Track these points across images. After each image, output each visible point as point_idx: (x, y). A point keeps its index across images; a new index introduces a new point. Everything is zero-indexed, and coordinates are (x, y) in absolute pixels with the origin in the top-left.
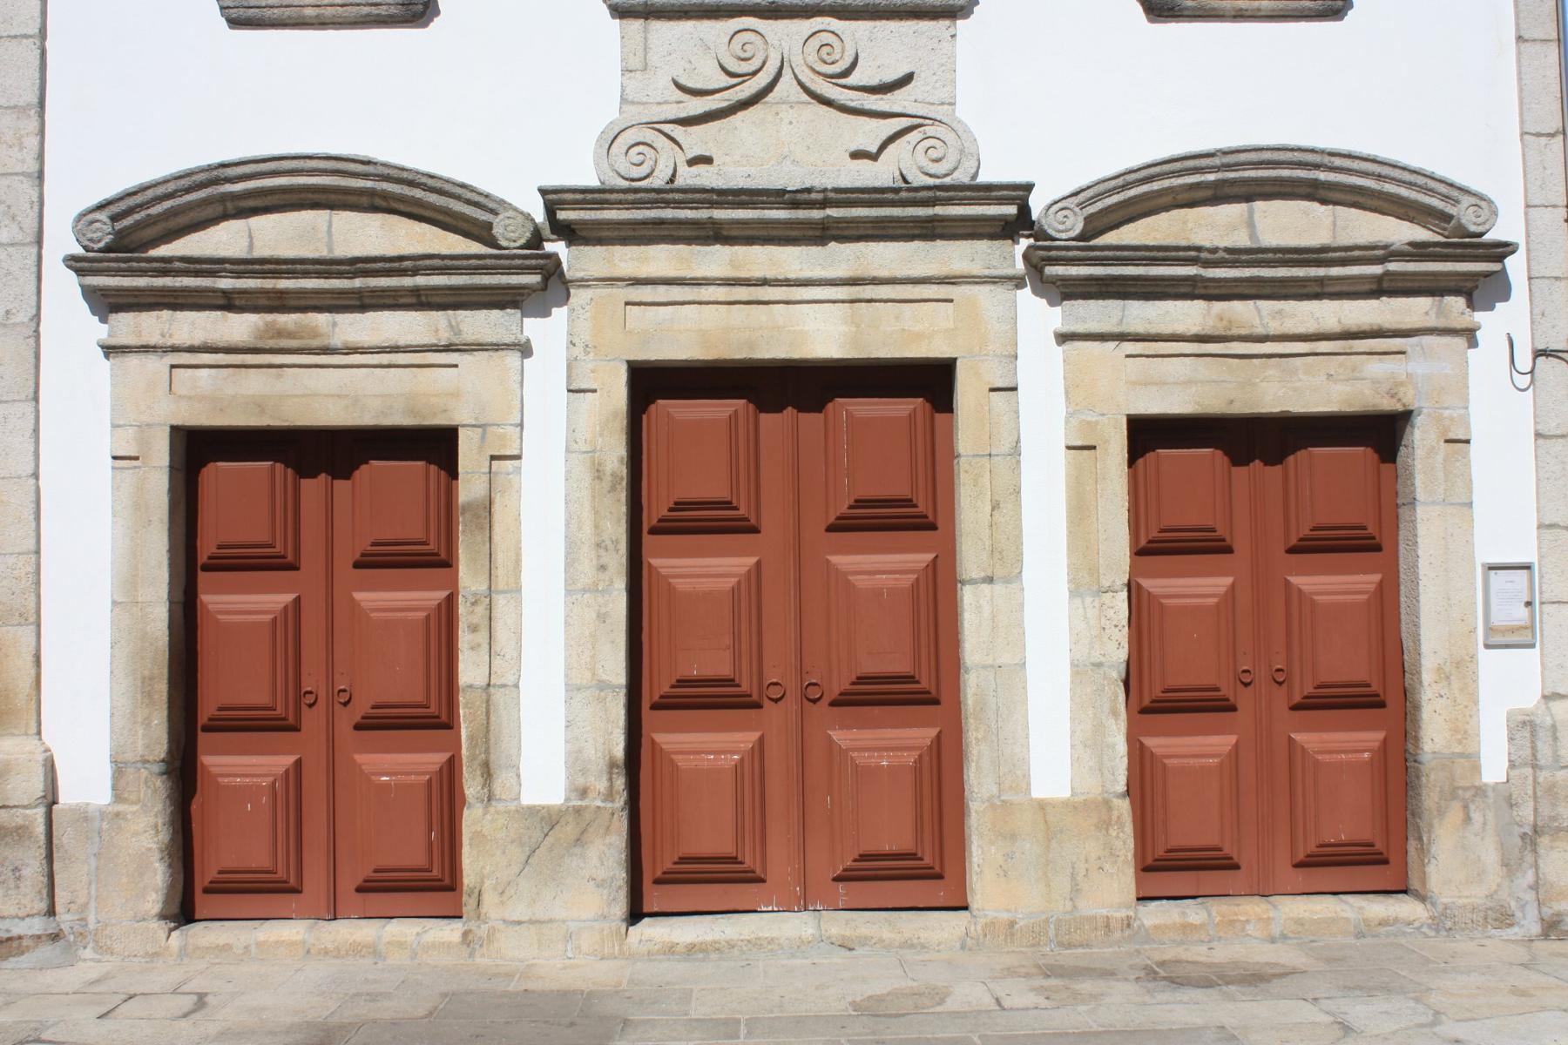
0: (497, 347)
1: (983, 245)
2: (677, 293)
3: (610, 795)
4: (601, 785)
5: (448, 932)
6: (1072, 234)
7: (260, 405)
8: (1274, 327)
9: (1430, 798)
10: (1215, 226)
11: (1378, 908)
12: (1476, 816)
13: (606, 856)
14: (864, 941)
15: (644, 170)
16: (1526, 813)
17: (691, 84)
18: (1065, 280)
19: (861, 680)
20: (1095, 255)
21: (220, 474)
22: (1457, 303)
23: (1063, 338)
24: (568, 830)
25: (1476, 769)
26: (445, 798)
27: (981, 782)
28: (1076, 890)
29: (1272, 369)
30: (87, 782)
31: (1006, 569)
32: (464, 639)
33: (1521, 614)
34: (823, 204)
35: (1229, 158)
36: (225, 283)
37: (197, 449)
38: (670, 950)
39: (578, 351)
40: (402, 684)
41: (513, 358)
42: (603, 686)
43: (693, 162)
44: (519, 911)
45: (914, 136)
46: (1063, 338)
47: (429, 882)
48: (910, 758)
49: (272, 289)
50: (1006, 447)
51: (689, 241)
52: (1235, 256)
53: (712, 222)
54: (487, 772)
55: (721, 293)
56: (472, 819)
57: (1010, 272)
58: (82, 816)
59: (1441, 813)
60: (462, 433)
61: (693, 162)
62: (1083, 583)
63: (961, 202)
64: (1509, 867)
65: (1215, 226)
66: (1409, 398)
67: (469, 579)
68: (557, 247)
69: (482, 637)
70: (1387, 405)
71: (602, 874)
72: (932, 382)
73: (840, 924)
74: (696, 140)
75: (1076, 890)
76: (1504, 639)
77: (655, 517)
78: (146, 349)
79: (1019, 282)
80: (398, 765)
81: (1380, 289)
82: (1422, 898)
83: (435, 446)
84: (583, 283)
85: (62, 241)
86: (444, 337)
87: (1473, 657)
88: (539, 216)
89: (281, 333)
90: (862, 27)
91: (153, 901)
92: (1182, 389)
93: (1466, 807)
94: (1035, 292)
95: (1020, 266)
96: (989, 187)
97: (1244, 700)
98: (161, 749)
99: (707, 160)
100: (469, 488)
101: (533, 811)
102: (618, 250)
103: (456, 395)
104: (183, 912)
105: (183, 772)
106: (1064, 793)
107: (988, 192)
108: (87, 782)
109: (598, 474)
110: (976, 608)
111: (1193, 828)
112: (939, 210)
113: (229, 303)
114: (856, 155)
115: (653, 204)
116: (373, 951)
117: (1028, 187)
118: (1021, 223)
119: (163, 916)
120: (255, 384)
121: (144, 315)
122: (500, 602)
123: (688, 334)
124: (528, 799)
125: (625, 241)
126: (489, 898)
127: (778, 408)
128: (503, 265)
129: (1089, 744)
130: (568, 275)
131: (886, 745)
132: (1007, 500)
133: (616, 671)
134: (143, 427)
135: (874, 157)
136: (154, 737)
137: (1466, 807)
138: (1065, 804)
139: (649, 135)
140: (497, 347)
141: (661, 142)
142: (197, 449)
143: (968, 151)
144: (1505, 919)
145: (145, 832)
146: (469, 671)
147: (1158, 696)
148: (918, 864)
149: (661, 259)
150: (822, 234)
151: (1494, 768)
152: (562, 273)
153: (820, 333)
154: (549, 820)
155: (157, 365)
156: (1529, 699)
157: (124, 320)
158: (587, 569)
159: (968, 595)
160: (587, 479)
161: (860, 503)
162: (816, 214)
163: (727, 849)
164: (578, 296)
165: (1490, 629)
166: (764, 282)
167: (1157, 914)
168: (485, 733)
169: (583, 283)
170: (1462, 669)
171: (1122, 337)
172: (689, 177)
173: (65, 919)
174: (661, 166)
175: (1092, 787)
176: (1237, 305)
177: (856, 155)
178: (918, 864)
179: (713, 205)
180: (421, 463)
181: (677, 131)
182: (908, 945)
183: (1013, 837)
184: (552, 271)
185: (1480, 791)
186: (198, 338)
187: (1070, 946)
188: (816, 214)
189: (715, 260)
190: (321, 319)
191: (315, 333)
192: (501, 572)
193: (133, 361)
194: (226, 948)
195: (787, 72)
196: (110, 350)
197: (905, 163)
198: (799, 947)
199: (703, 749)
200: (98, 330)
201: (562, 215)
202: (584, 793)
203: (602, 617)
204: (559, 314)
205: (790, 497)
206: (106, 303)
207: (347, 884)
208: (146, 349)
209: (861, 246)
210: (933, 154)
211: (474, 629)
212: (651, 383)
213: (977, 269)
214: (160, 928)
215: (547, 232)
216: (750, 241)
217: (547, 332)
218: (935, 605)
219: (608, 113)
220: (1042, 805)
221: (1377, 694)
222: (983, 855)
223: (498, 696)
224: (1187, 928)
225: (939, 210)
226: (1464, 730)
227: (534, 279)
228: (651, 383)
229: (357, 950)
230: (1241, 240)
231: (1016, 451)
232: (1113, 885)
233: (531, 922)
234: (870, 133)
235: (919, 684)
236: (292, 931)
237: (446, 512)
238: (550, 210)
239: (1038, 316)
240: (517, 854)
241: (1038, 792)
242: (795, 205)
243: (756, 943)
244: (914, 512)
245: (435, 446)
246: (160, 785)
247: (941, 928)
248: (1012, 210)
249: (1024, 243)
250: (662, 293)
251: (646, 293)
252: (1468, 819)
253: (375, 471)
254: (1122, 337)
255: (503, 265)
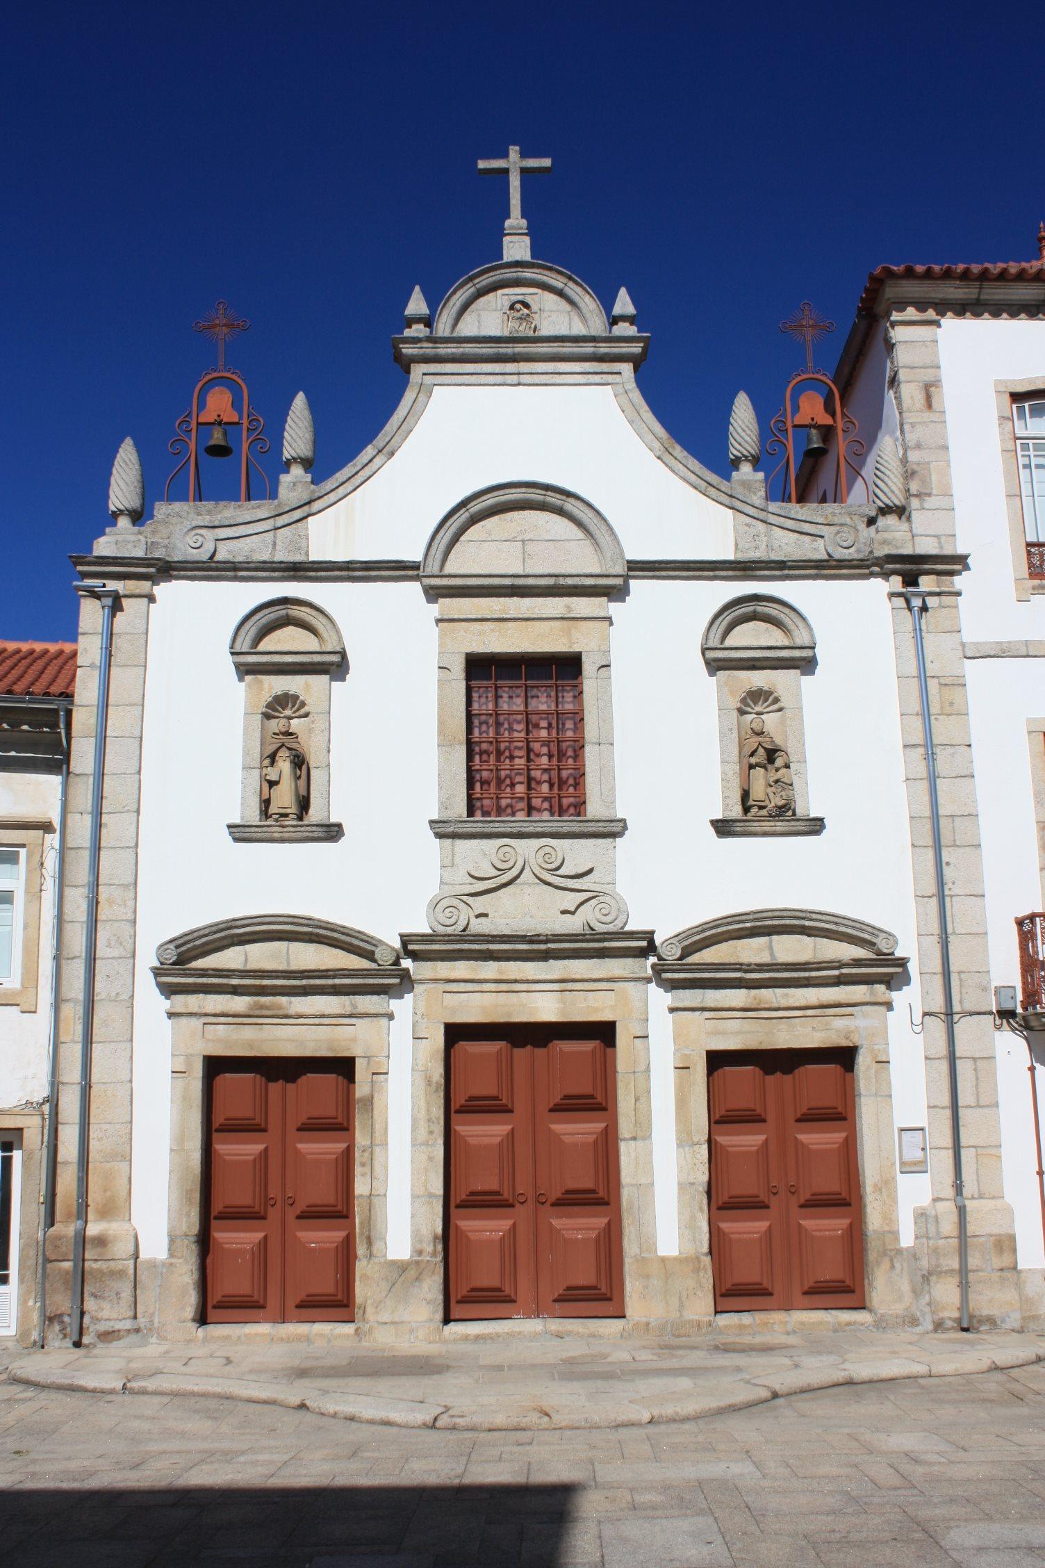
0: (376, 1015)
1: (629, 961)
2: (470, 987)
3: (434, 1254)
4: (430, 1249)
5: (348, 1329)
6: (678, 956)
7: (250, 1044)
8: (784, 1003)
9: (872, 1256)
10: (751, 951)
11: (845, 1316)
12: (897, 1265)
13: (432, 1287)
14: (569, 1333)
15: (452, 921)
16: (924, 1263)
17: (477, 875)
18: (672, 980)
19: (568, 1192)
20: (688, 967)
21: (227, 1079)
22: (881, 988)
23: (672, 1010)
24: (412, 1273)
25: (897, 1239)
26: (346, 1256)
27: (631, 1247)
28: (681, 1306)
29: (783, 1025)
30: (155, 1247)
31: (643, 1133)
32: (358, 1170)
33: (920, 1154)
34: (546, 942)
35: (757, 915)
36: (235, 982)
37: (215, 1066)
38: (466, 1338)
39: (418, 1017)
40: (322, 1193)
41: (384, 1021)
42: (431, 1195)
43: (478, 916)
44: (385, 1317)
45: (593, 902)
46: (672, 1010)
47: (338, 1303)
48: (593, 1234)
49: (258, 984)
50: (643, 1068)
51: (476, 959)
52: (761, 967)
53: (488, 950)
54: (370, 1242)
55: (493, 987)
56: (361, 1267)
57: (643, 975)
58: (152, 1264)
59: (878, 1264)
60: (358, 1061)
61: (478, 916)
62: (684, 1140)
63: (618, 940)
64: (916, 1293)
65: (751, 951)
66: (855, 1040)
67: (361, 1139)
68: (407, 963)
69: (367, 1169)
70: (844, 1043)
71: (430, 1297)
72: (604, 1032)
73: (555, 1325)
74: (479, 904)
75: (681, 1306)
76: (912, 1168)
77: (458, 1104)
78: (191, 1015)
79: (649, 980)
80: (319, 1238)
81: (839, 981)
82: (871, 1311)
83: (344, 1067)
84: (421, 981)
85: (147, 959)
86: (348, 1010)
87: (894, 1178)
88: (397, 944)
89: (262, 1007)
90: (566, 843)
91: (190, 1311)
92: (735, 1036)
93: (892, 1260)
94: (658, 985)
95: (650, 972)
96: (632, 933)
97: (774, 1202)
98: (195, 1229)
99: (486, 915)
100: (361, 1088)
101: (393, 1263)
102: (439, 964)
103: (354, 1040)
104: (202, 1319)
105: (204, 1241)
106: (676, 1253)
107: (632, 935)
108: (155, 1247)
109: (429, 1082)
110: (627, 1153)
111: (747, 1272)
112: (606, 944)
113: (235, 991)
114: (563, 912)
115: (458, 942)
116: (307, 1339)
117: (653, 933)
118: (651, 948)
119: (194, 1320)
120: (248, 1033)
121: (190, 996)
122: (377, 1150)
123: (477, 1007)
124: (390, 1257)
125: (443, 959)
126: (370, 1310)
127: (523, 1046)
128: (379, 974)
129: (687, 1225)
130: (413, 977)
131: (580, 1227)
132: (643, 1095)
133: (438, 1187)
134: (188, 1057)
135: (573, 913)
136: (191, 1222)
137: (892, 1260)
138: (675, 1259)
139: (455, 902)
140: (376, 1015)
141: (462, 906)
142: (215, 1066)
143: (623, 911)
144: (914, 1322)
145: (186, 1274)
146: (361, 1187)
147: (724, 1199)
148: (598, 1293)
149: (461, 969)
150: (545, 956)
151: (907, 1239)
152: (410, 976)
153: (545, 1007)
154: (402, 1267)
155: (196, 1023)
156: (925, 1201)
157: (179, 999)
158: (423, 1133)
159: (623, 1147)
160: (423, 1085)
161: (566, 1097)
162: (543, 947)
163: (495, 1283)
164: (419, 988)
165: (902, 1163)
166: (516, 981)
167: (724, 1320)
168: (369, 1220)
169: (421, 981)
170: (888, 1185)
171: (703, 1009)
172: (478, 926)
173: (142, 1321)
174: (462, 917)
175: (690, 1250)
176: (763, 991)
177: (563, 912)
178: (598, 1293)
179: (489, 942)
180: (334, 1076)
181: (470, 900)
182: (593, 1336)
183: (648, 1276)
184: (405, 975)
185: (899, 1251)
186: (218, 1010)
187: (678, 1336)
188: (543, 947)
189: (490, 969)
190: (283, 1000)
191: (280, 1007)
192: (377, 1134)
193: (184, 1020)
194: (228, 1337)
195: (527, 870)
196: (171, 1015)
197: (589, 917)
198: (535, 1336)
199: (485, 1229)
200: (165, 1004)
201: (411, 947)
202: (420, 1253)
203: (431, 1159)
204: (409, 997)
205: (530, 1092)
206: (169, 991)
207: (291, 1303)
208: (191, 1015)
209: (566, 962)
210: (603, 911)
211: (363, 1165)
212: (456, 1033)
213: (626, 974)
214: (193, 1326)
215: (402, 954)
216: (508, 959)
217: (403, 1007)
218: (606, 1152)
219: (434, 890)
220: (663, 1260)
221: (844, 1199)
222: (632, 1286)
223: (375, 1200)
224: (741, 1327)
225: (606, 944)
226: (890, 1218)
227: (397, 981)
228: (456, 1033)
229: (299, 1338)
230: (765, 958)
231: (648, 1070)
232: (701, 1305)
233: (392, 1323)
234: (570, 900)
235: (599, 1194)
236: (264, 1328)
237: (347, 1102)
238: (404, 944)
239: (659, 998)
240: (385, 1286)
241: (660, 1253)
242: (531, 942)
243: (511, 1335)
244: (596, 1101)
245: (344, 1067)
246: (194, 1248)
247: (610, 1327)
248: (644, 944)
249: (653, 960)
250: (462, 987)
251: (454, 987)
252: (893, 1267)
253: (311, 1079)
254: (703, 1009)
255: (379, 974)
